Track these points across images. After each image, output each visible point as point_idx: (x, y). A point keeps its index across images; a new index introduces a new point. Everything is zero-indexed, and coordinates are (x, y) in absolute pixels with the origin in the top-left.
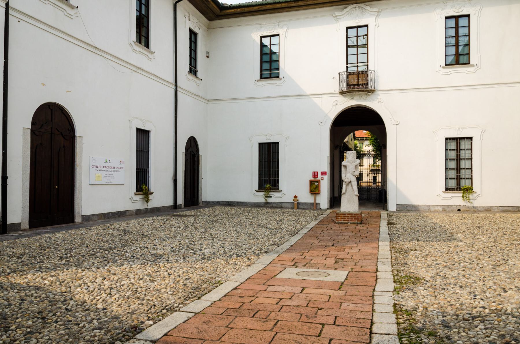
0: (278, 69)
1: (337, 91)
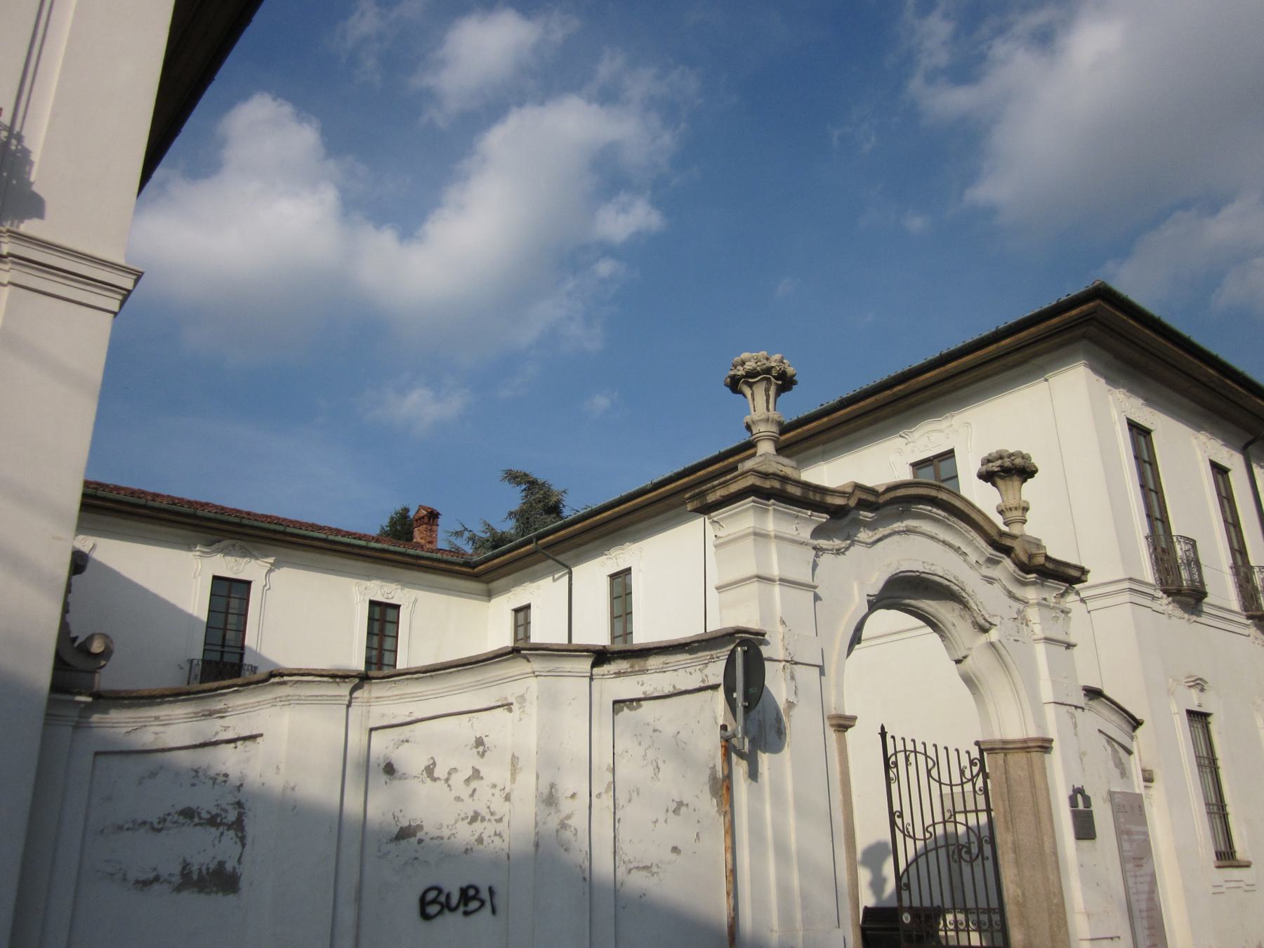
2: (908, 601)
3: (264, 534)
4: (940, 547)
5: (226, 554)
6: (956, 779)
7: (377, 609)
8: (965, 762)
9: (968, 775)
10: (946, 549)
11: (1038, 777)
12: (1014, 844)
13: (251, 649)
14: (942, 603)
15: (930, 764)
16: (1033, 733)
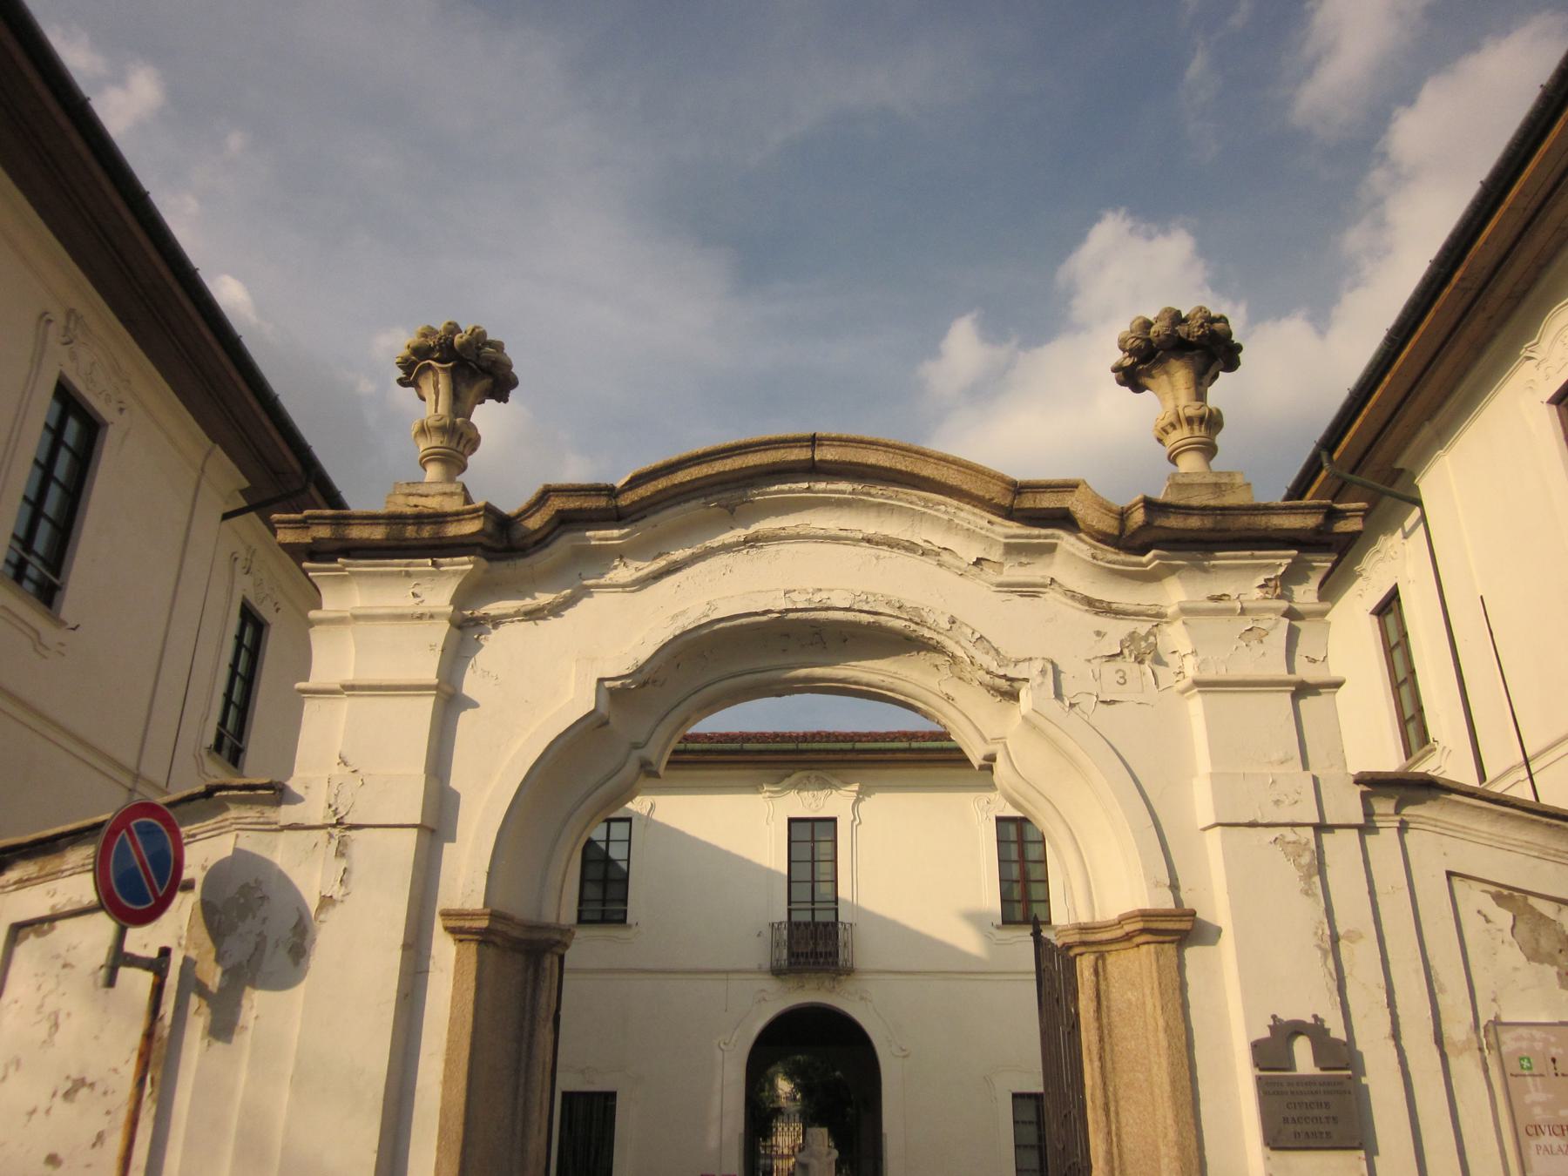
0: (625, 901)
1: (767, 966)
2: (803, 672)
3: (831, 757)
4: (866, 551)
5: (800, 791)
10: (884, 552)
13: (845, 901)
14: (904, 658)
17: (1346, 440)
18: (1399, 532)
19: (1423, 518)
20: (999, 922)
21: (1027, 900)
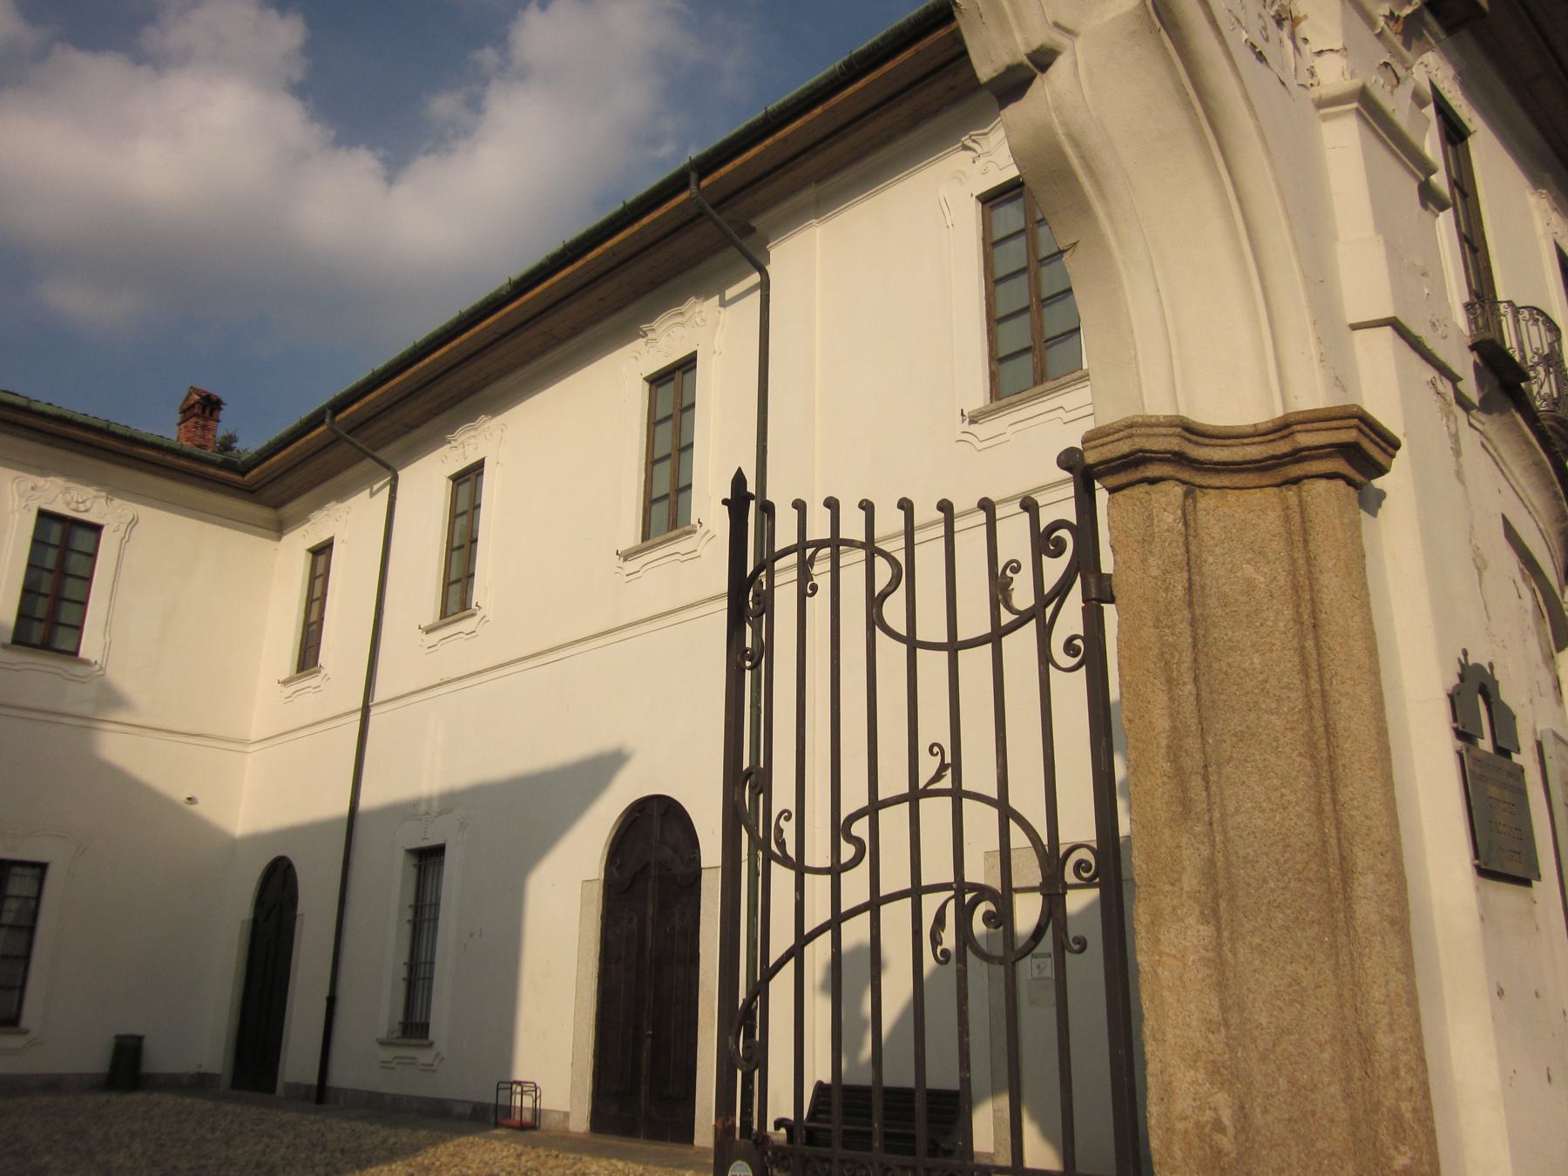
6: (975, 619)
7: (56, 531)
8: (1015, 540)
9: (1023, 595)
11: (1331, 584)
12: (1210, 873)
15: (883, 572)
16: (1312, 395)
17: (729, 167)
18: (716, 298)
19: (765, 286)
20: (8, 639)
21: (53, 622)
